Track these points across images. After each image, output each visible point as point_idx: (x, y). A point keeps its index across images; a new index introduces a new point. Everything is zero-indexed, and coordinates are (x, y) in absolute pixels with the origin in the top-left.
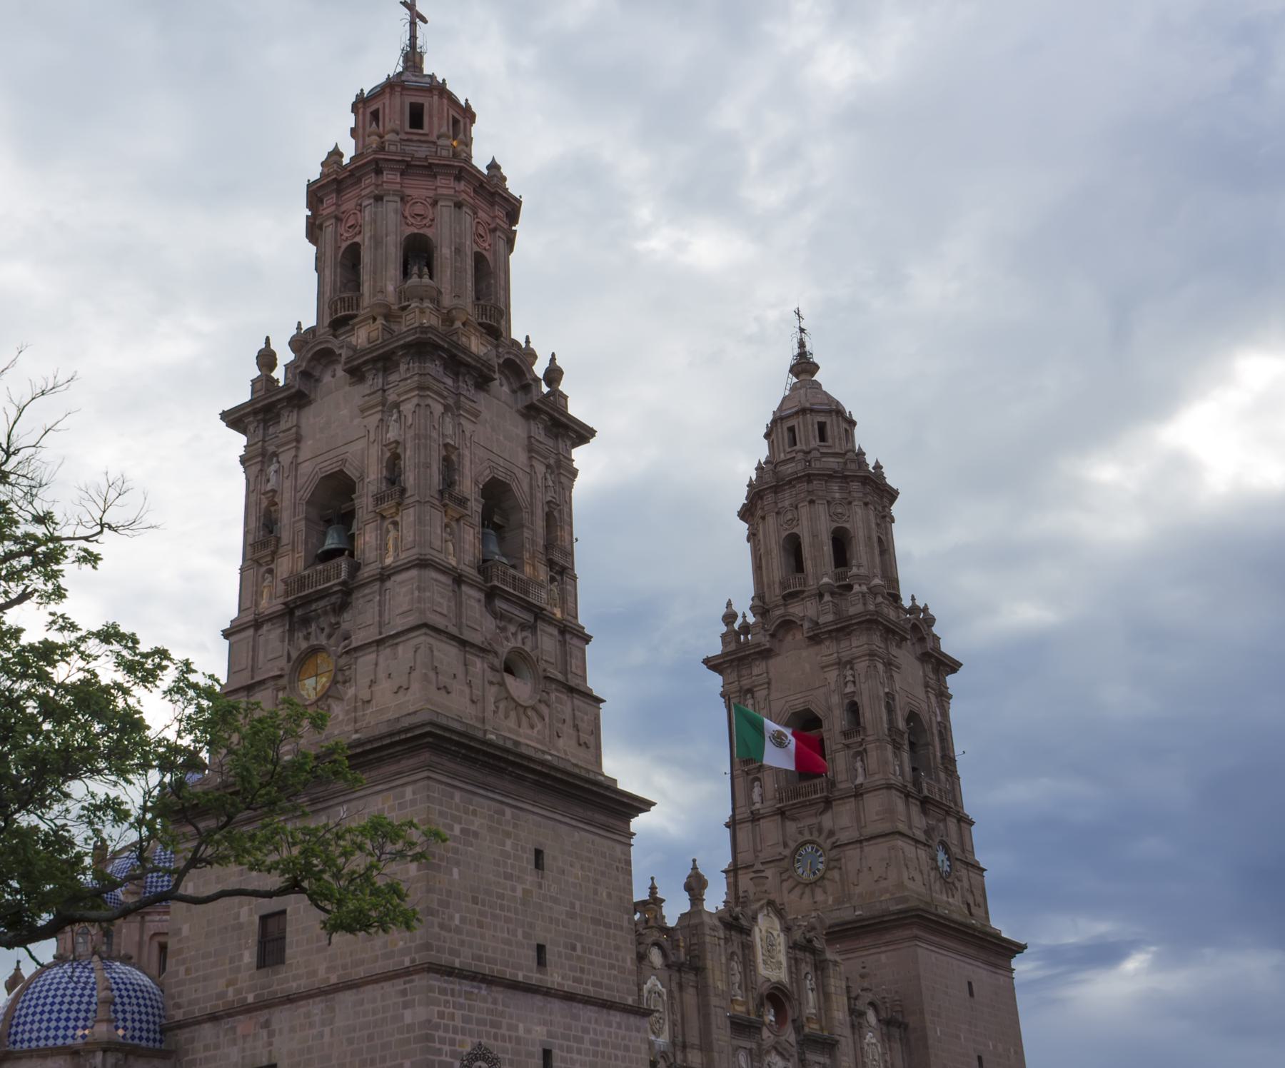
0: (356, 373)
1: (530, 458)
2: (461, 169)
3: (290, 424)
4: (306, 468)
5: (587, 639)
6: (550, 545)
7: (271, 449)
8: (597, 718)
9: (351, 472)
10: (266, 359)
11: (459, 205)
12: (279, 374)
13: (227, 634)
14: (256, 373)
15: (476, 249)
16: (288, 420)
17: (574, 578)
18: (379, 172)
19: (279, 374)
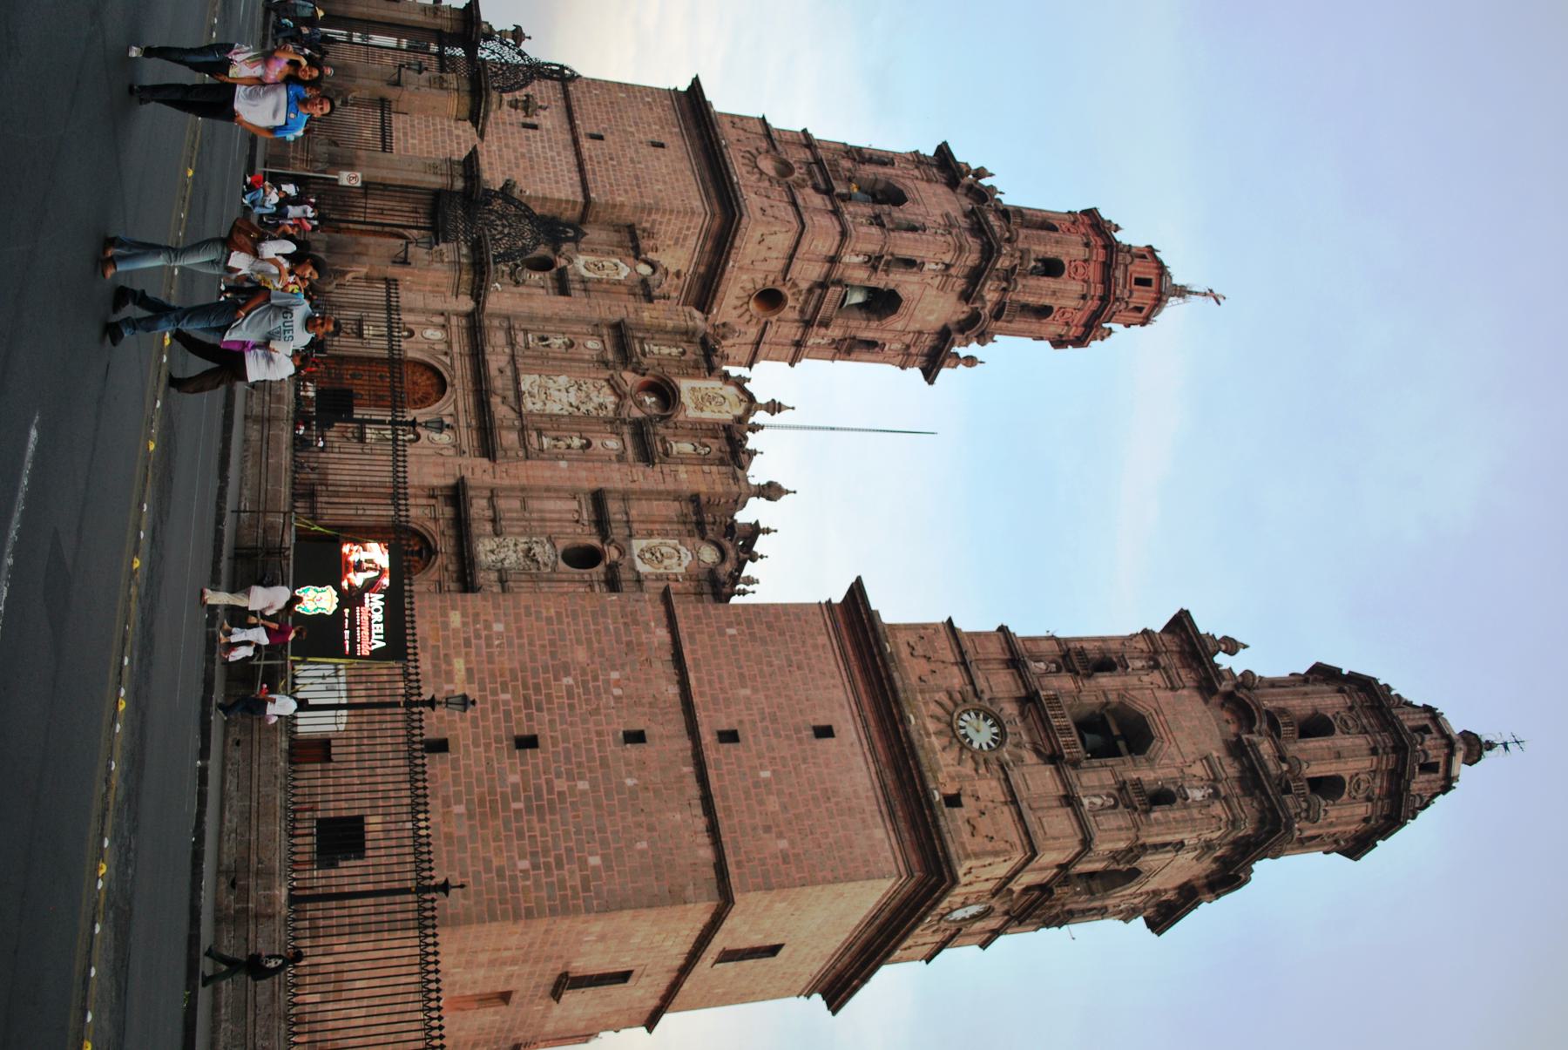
1: (1147, 893)
3: (1184, 679)
10: (1232, 646)
16: (1187, 676)
17: (1036, 930)
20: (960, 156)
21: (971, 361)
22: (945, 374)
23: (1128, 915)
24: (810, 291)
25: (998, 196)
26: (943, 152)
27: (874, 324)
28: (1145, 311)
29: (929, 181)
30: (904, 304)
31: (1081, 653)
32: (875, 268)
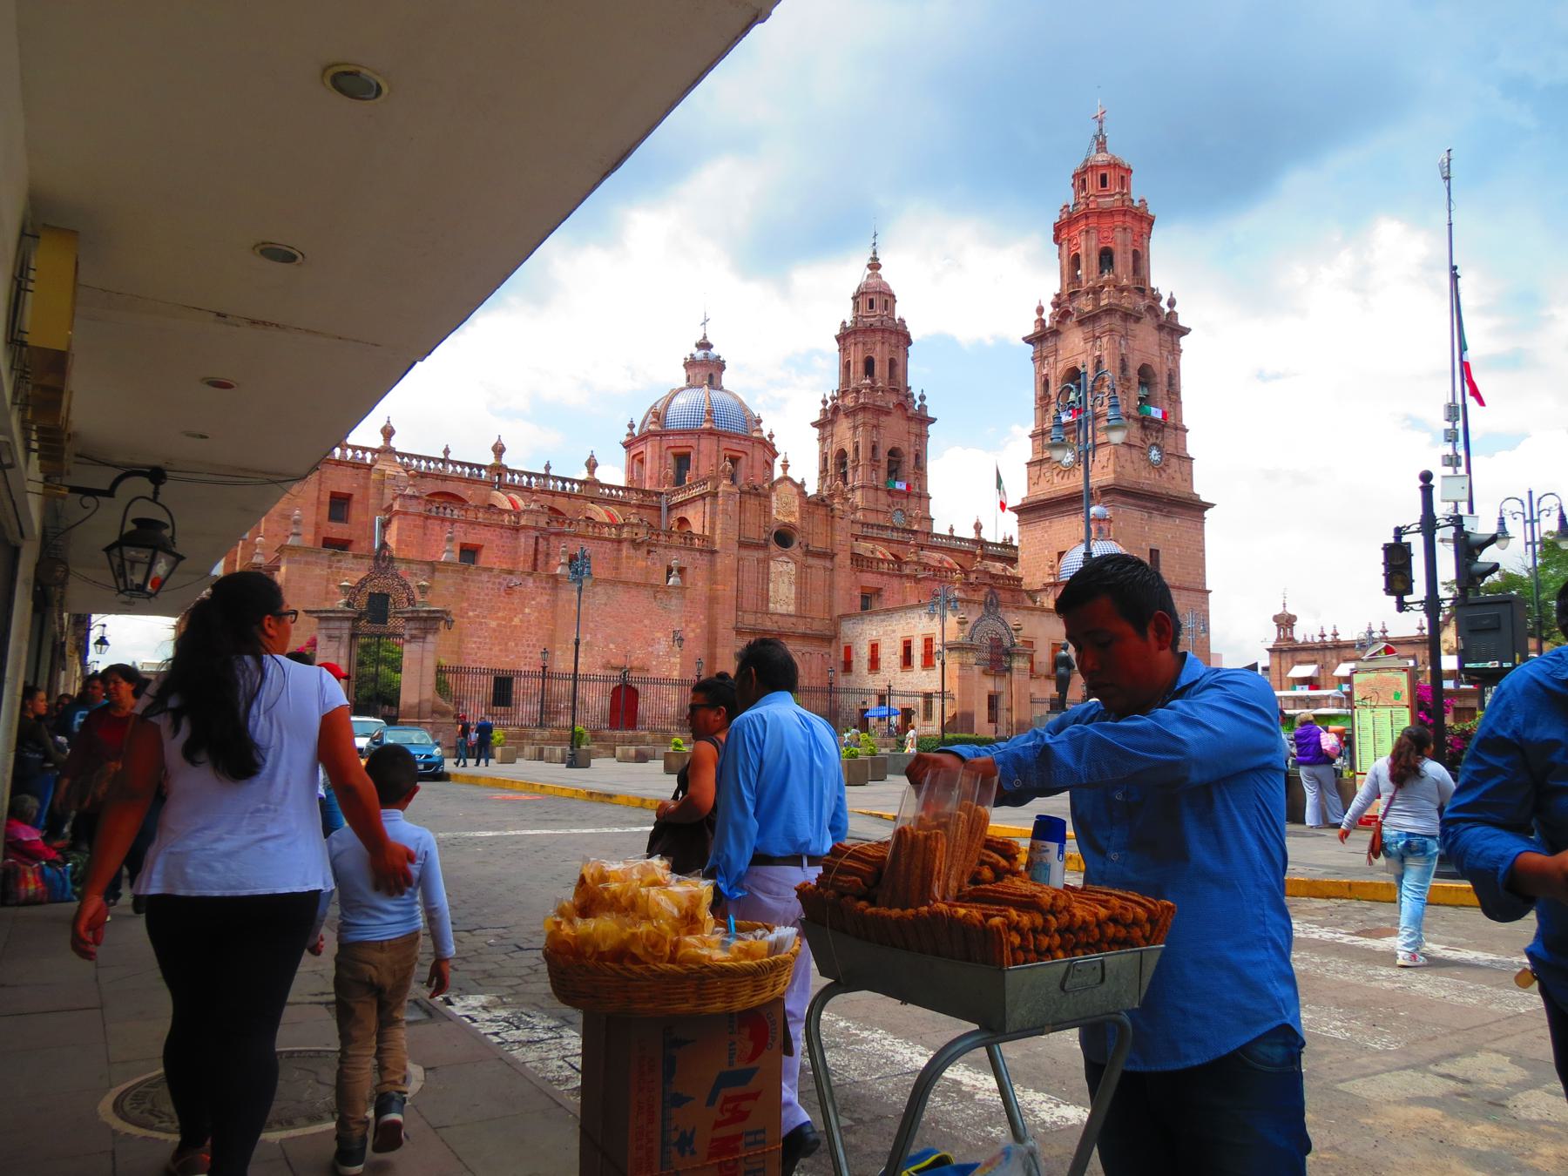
0: (1081, 323)
2: (1126, 211)
4: (1060, 365)
5: (1187, 431)
6: (1170, 384)
7: (1044, 354)
8: (1191, 467)
9: (1079, 366)
10: (1040, 310)
11: (1125, 229)
12: (1046, 316)
13: (1031, 437)
14: (1036, 317)
15: (1133, 248)
16: (1050, 343)
17: (1181, 403)
18: (1087, 218)
19: (1046, 316)
20: (817, 417)
21: (922, 398)
22: (930, 414)
23: (1176, 352)
24: (892, 496)
25: (835, 394)
26: (814, 425)
27: (906, 459)
28: (888, 298)
29: (832, 435)
30: (896, 446)
31: (1041, 399)
32: (879, 467)
